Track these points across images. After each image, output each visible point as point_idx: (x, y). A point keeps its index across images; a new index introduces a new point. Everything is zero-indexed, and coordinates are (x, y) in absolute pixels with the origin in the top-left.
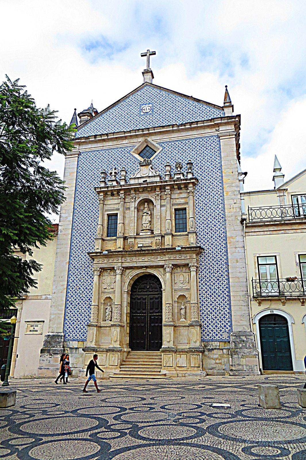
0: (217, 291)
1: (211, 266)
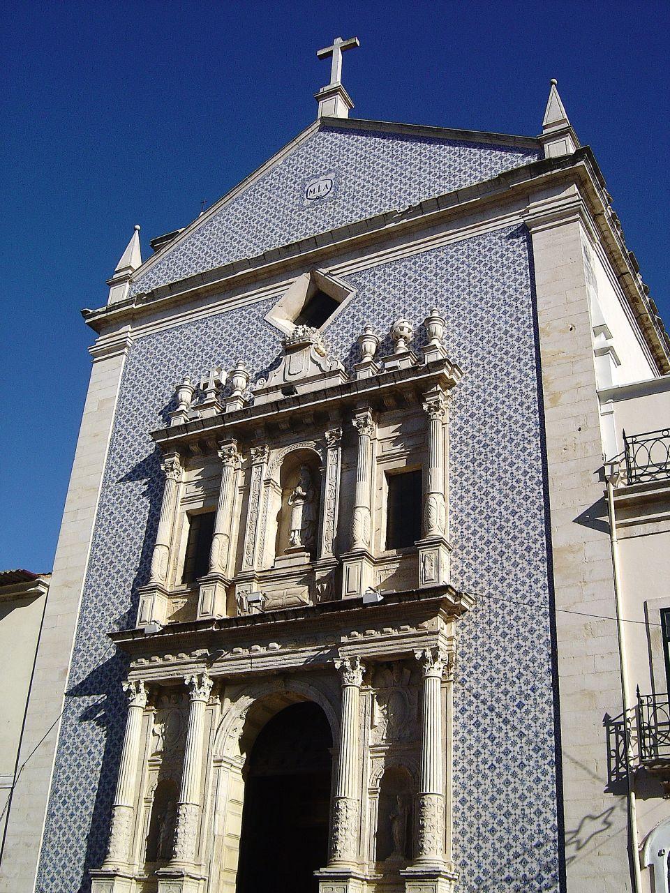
1: (498, 657)
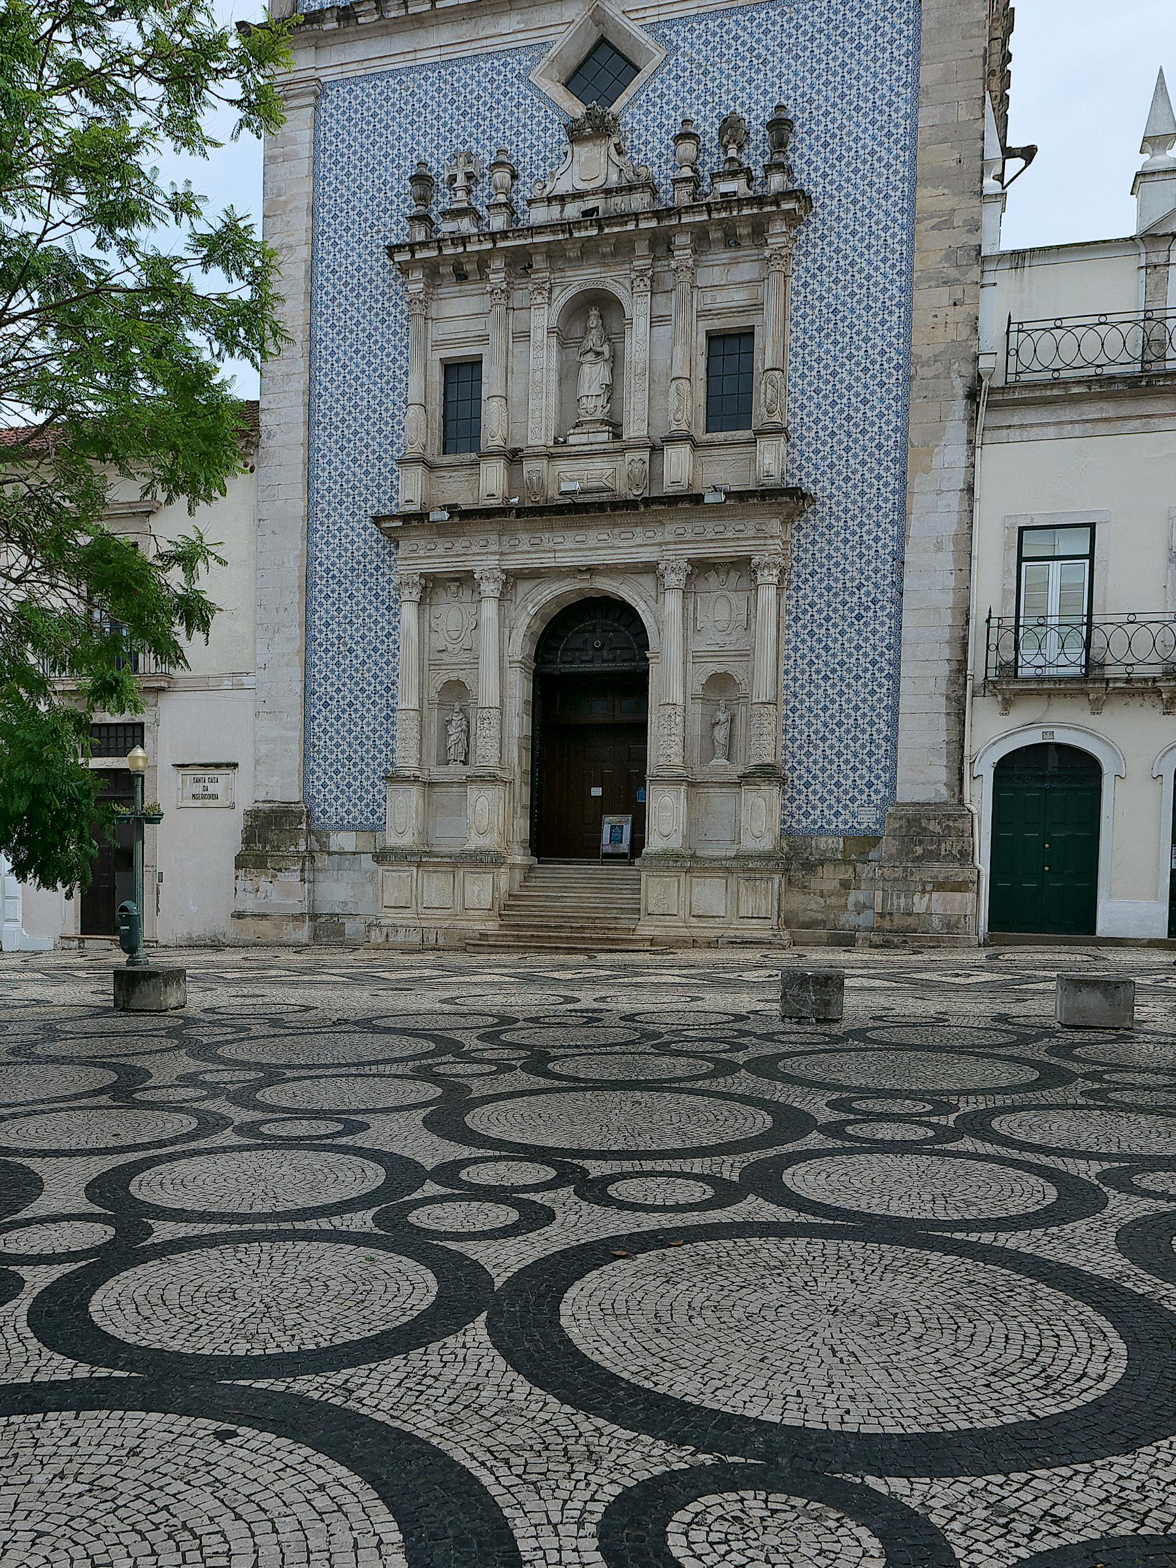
1: (837, 564)
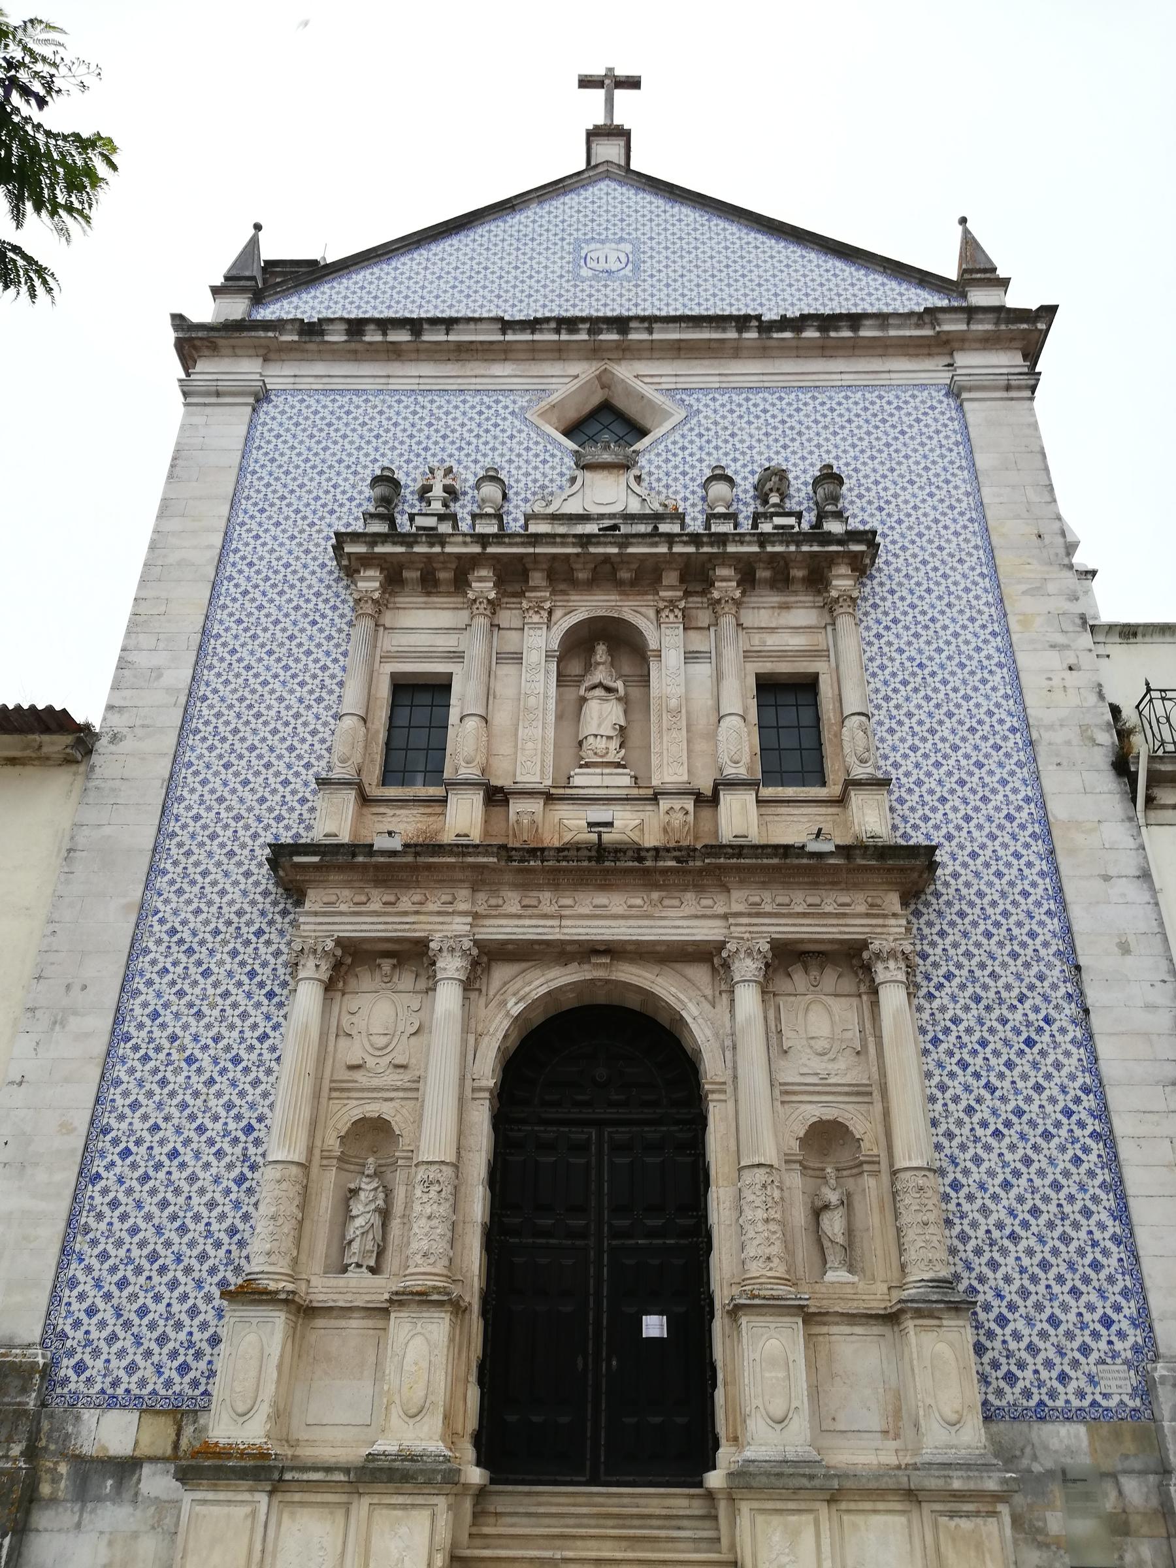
0: (1035, 1107)
1: (982, 966)
